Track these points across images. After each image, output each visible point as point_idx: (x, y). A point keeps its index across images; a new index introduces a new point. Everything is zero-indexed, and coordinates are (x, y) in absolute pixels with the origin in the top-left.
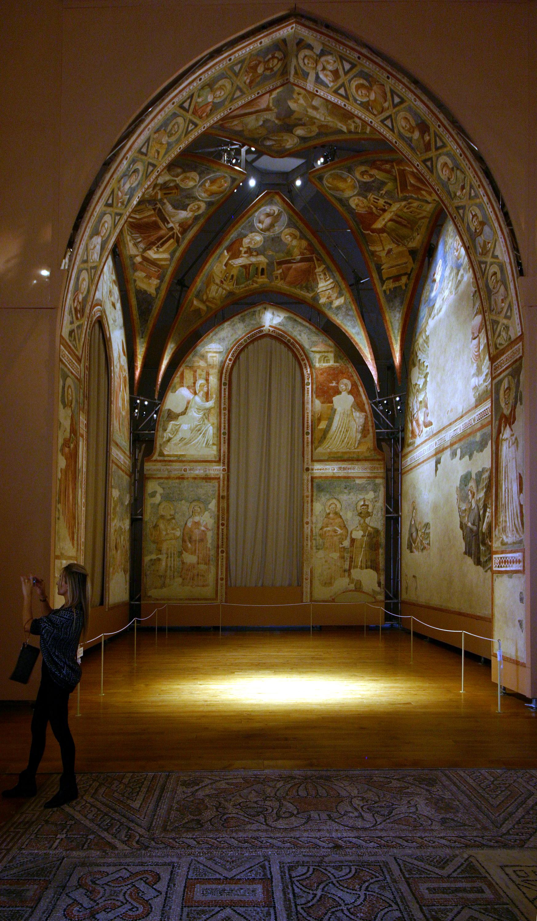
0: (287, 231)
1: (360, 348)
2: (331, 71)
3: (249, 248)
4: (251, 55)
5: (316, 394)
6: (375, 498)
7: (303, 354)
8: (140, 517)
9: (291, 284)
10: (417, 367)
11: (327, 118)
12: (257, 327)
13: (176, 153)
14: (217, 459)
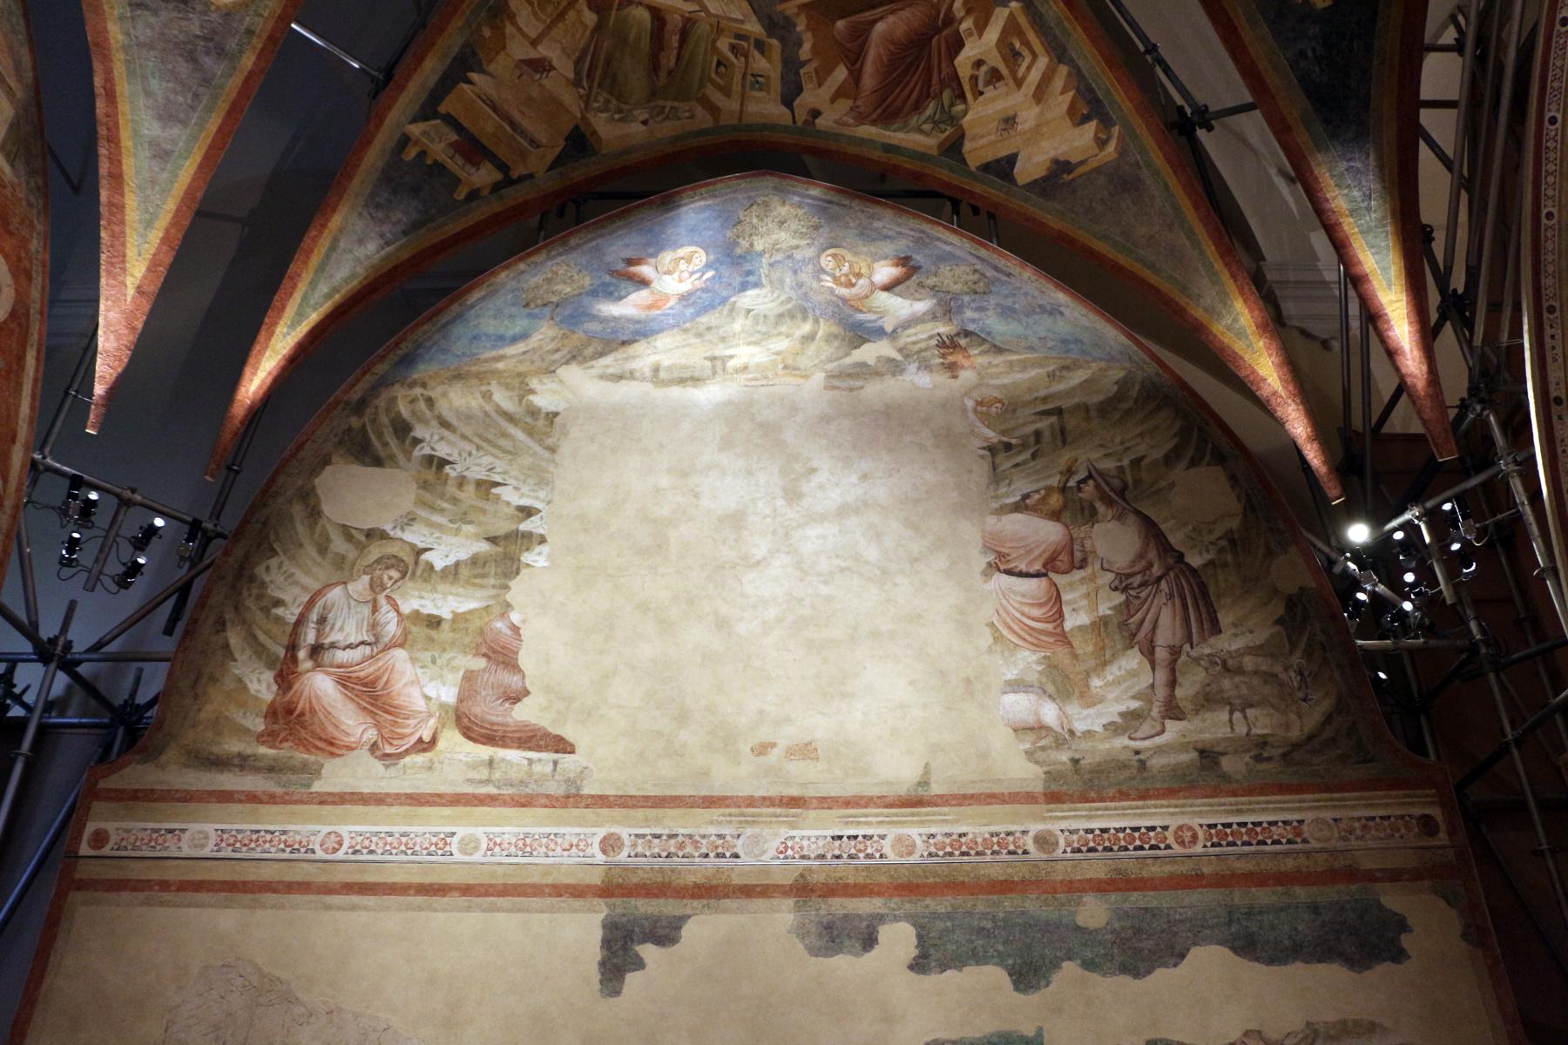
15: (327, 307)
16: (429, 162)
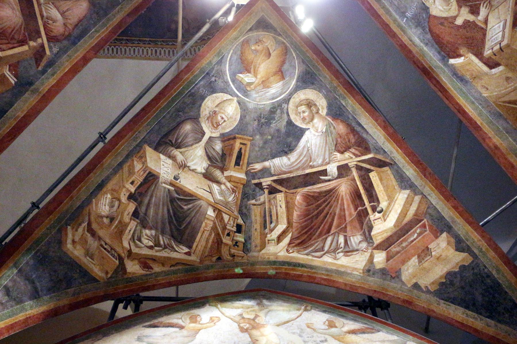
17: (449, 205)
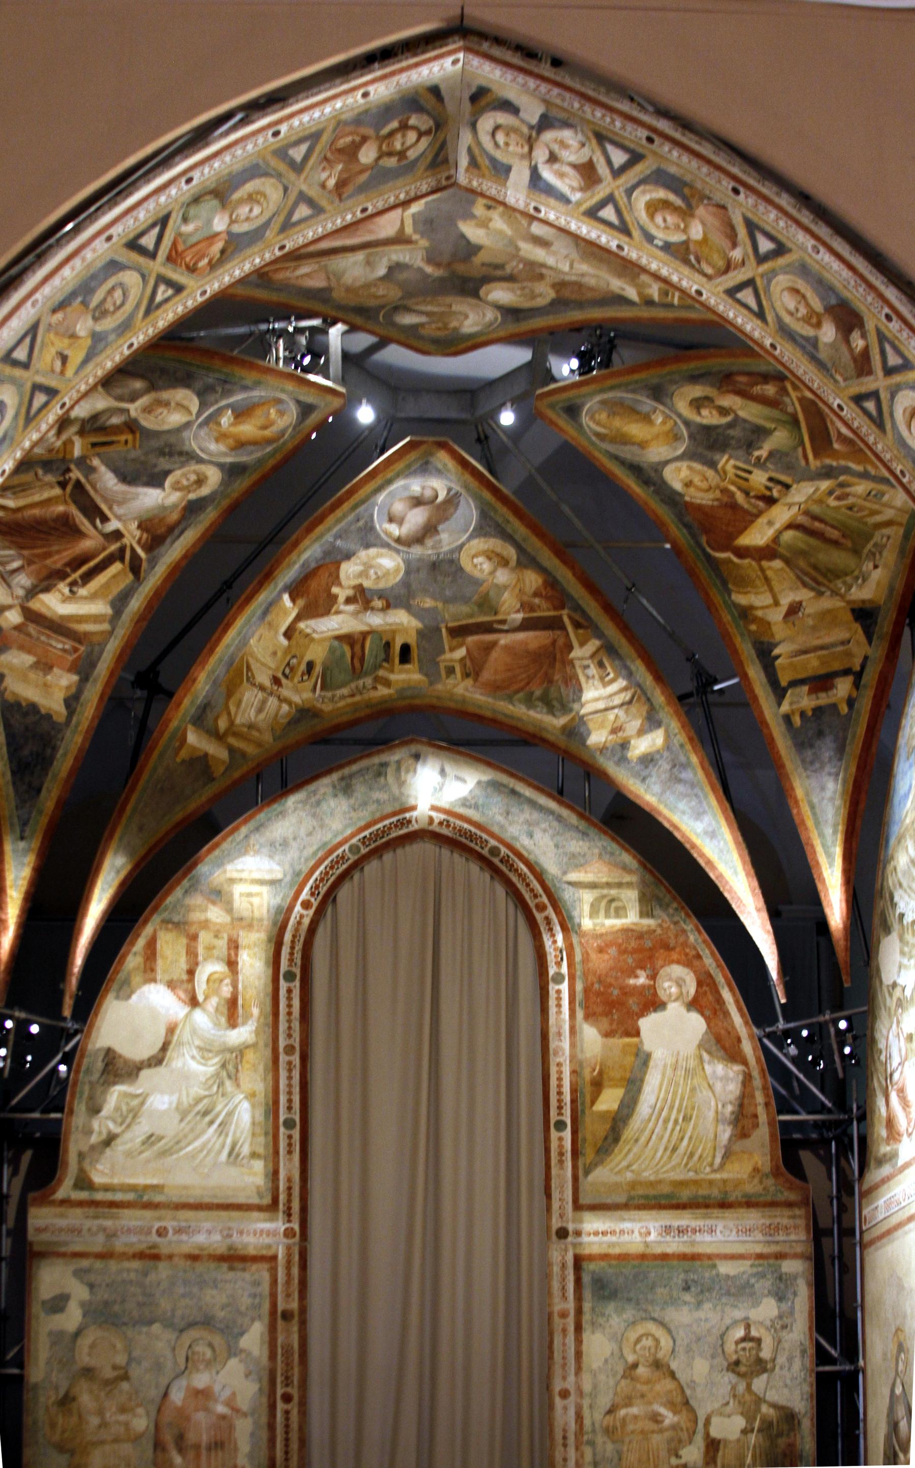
0: (479, 544)
1: (721, 876)
2: (574, 166)
3: (360, 589)
4: (339, 124)
5: (586, 1008)
6: (780, 1317)
7: (540, 890)
8: (15, 1371)
9: (495, 688)
10: (894, 936)
11: (576, 265)
12: (389, 809)
13: (118, 359)
14: (267, 1200)
15: (840, 837)
16: (810, 713)
17: (112, 665)
